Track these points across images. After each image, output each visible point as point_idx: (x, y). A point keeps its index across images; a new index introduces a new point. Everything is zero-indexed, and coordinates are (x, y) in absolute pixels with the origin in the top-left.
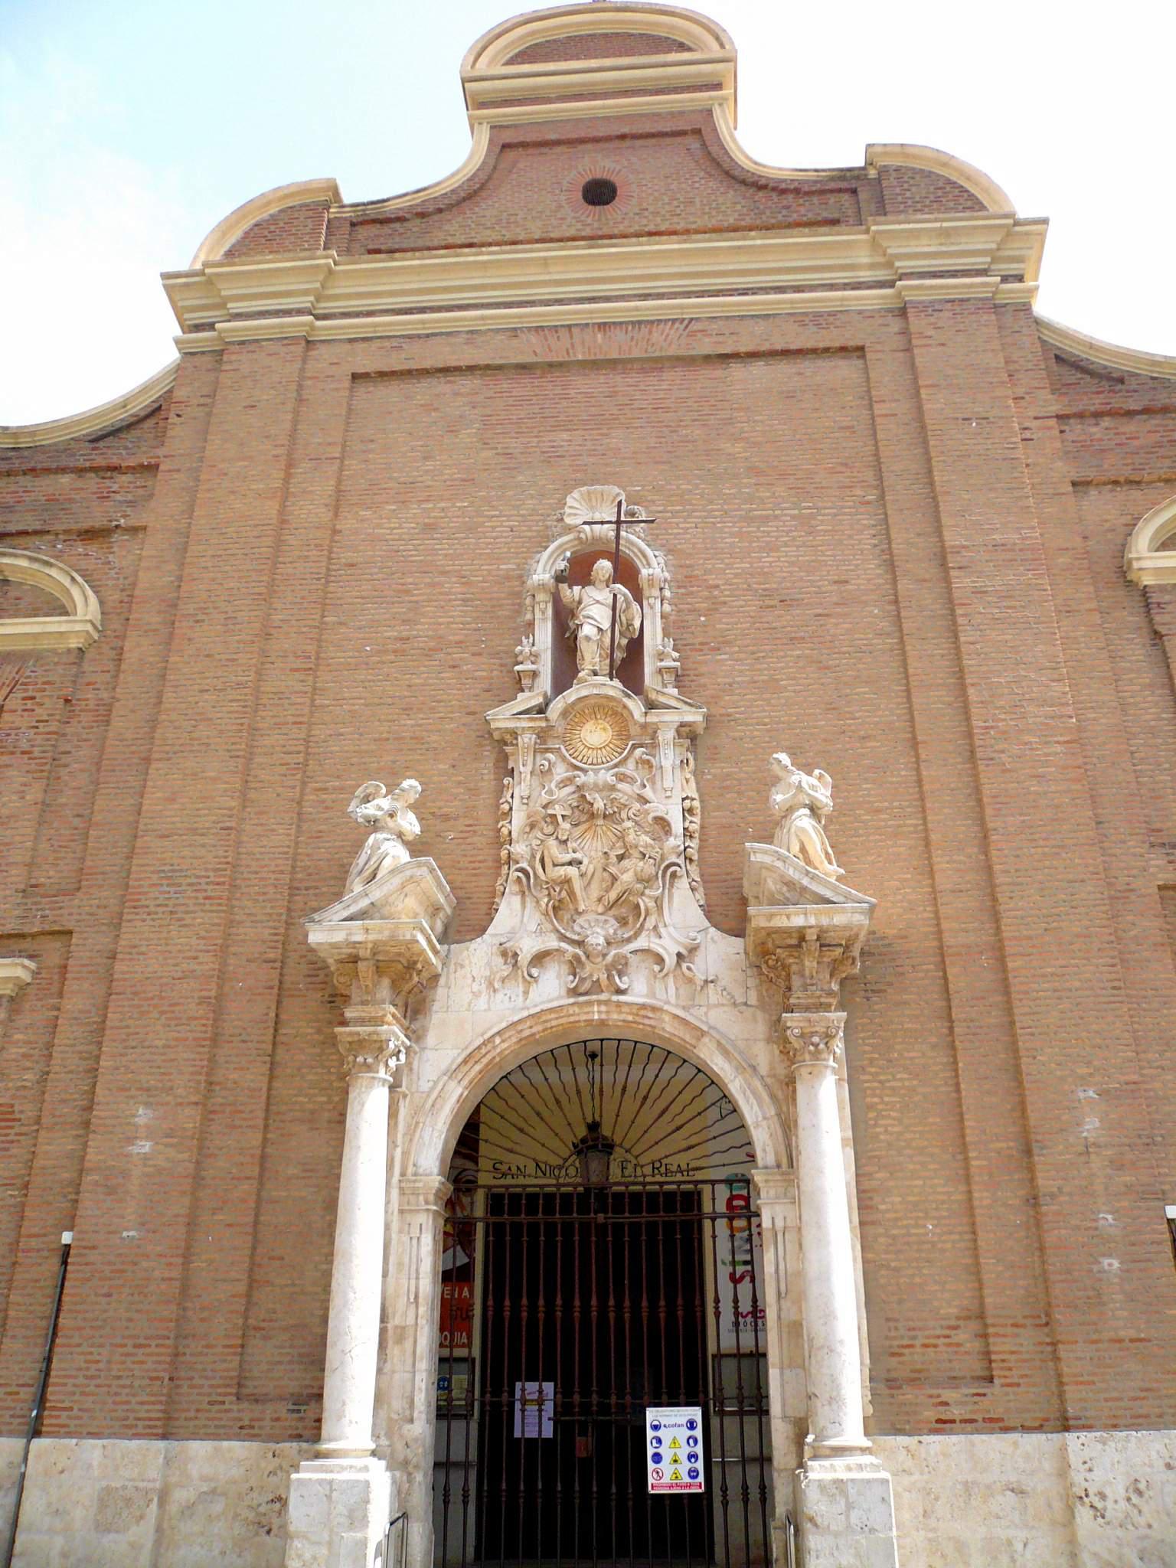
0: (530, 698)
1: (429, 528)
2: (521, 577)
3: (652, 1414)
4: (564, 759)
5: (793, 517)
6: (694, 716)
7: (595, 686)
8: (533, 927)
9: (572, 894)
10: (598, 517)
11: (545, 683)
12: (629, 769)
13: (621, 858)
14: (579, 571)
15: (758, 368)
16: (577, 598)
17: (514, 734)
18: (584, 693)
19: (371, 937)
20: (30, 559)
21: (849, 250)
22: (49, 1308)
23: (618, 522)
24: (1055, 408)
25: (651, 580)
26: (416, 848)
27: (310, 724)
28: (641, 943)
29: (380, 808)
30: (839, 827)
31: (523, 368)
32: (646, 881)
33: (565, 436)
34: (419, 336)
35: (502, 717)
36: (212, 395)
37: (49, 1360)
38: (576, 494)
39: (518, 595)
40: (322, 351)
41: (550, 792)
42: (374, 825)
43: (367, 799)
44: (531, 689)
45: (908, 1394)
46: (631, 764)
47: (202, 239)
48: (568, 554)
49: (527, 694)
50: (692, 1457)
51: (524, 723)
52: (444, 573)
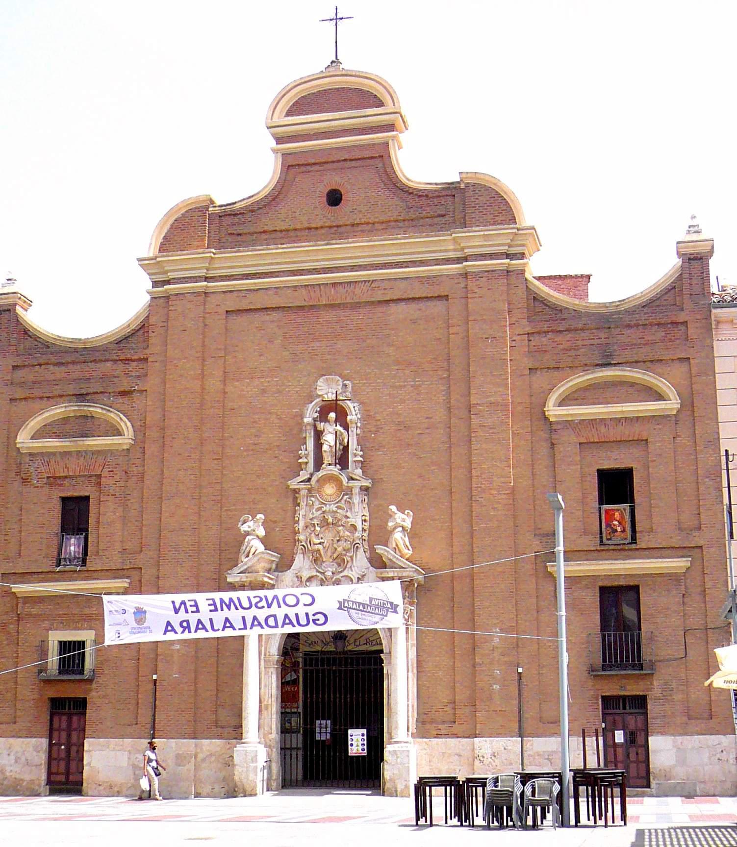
1: (264, 391)
3: (350, 731)
5: (412, 386)
6: (367, 483)
8: (307, 567)
9: (320, 555)
12: (342, 504)
13: (338, 541)
15: (402, 306)
19: (249, 579)
20: (102, 408)
21: (443, 243)
22: (152, 700)
24: (528, 329)
26: (263, 541)
27: (221, 483)
28: (345, 573)
29: (249, 527)
30: (413, 534)
31: (301, 308)
32: (348, 550)
33: (318, 344)
34: (254, 290)
35: (293, 484)
36: (167, 321)
37: (154, 716)
38: (321, 380)
40: (212, 299)
41: (313, 514)
42: (247, 534)
43: (244, 522)
45: (428, 726)
46: (343, 502)
47: (152, 233)
50: (363, 744)
51: (302, 486)
52: (270, 413)
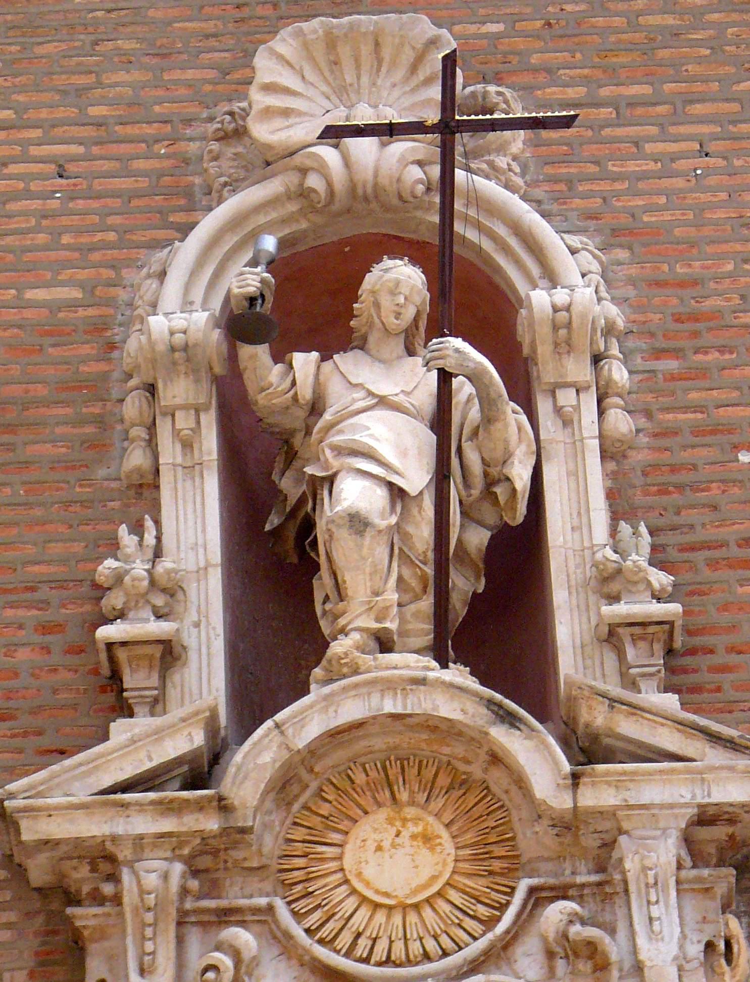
0: (158, 735)
2: (98, 328)
4: (284, 944)
7: (389, 686)
10: (364, 115)
11: (206, 677)
14: (308, 301)
16: (306, 392)
17: (104, 859)
18: (351, 710)
23: (447, 129)
25: (563, 322)
35: (64, 802)
38: (284, 43)
39: (96, 388)
44: (157, 704)
48: (269, 243)
49: (141, 723)
